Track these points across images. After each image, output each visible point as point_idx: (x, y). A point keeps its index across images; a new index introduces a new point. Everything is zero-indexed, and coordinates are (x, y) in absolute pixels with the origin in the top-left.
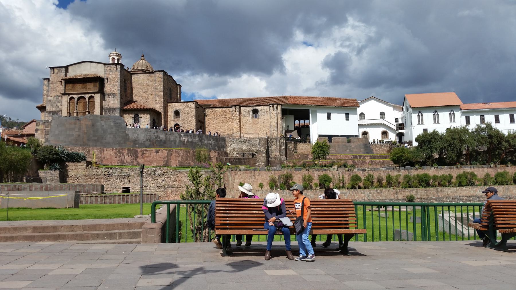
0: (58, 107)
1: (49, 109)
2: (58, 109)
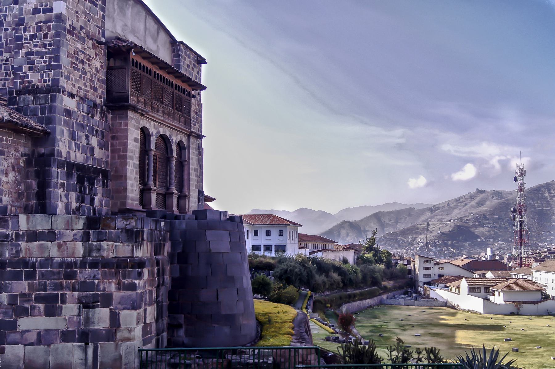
0: (92, 149)
1: (64, 154)
2: (90, 163)
